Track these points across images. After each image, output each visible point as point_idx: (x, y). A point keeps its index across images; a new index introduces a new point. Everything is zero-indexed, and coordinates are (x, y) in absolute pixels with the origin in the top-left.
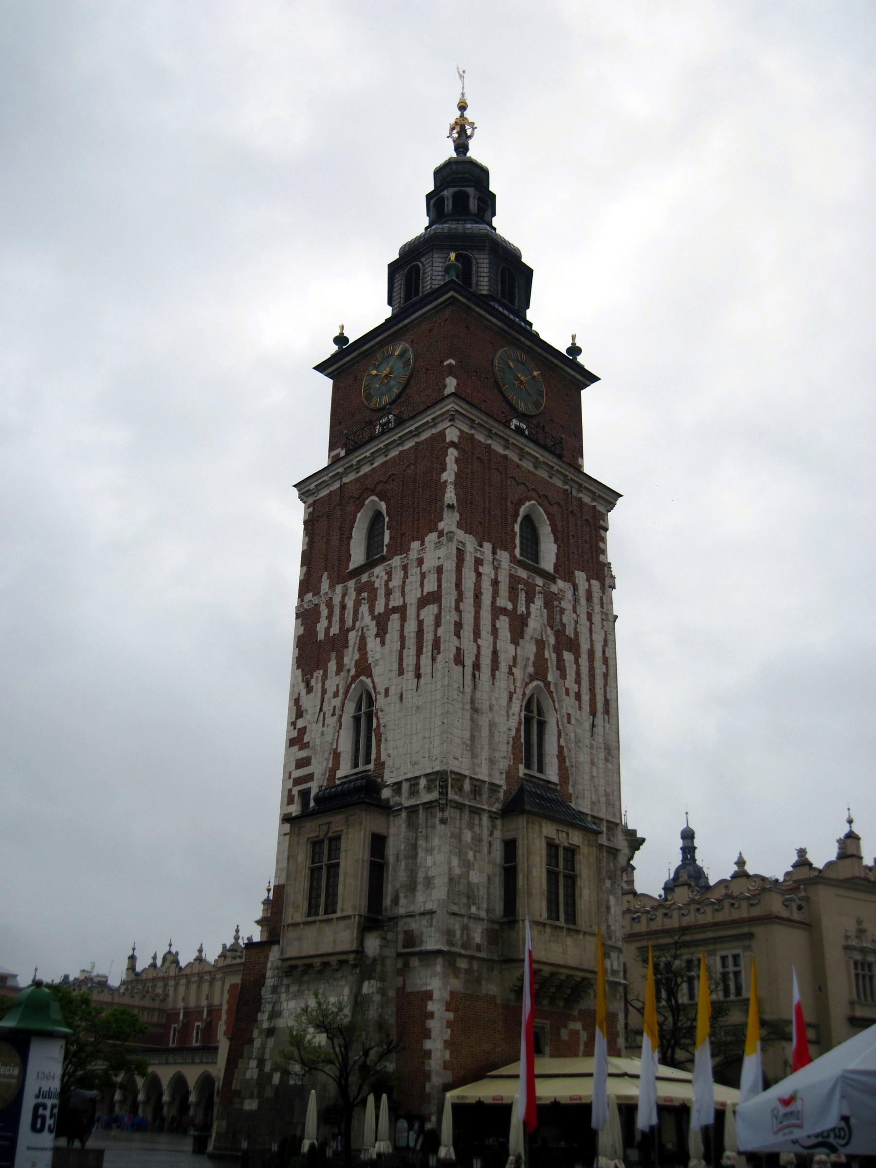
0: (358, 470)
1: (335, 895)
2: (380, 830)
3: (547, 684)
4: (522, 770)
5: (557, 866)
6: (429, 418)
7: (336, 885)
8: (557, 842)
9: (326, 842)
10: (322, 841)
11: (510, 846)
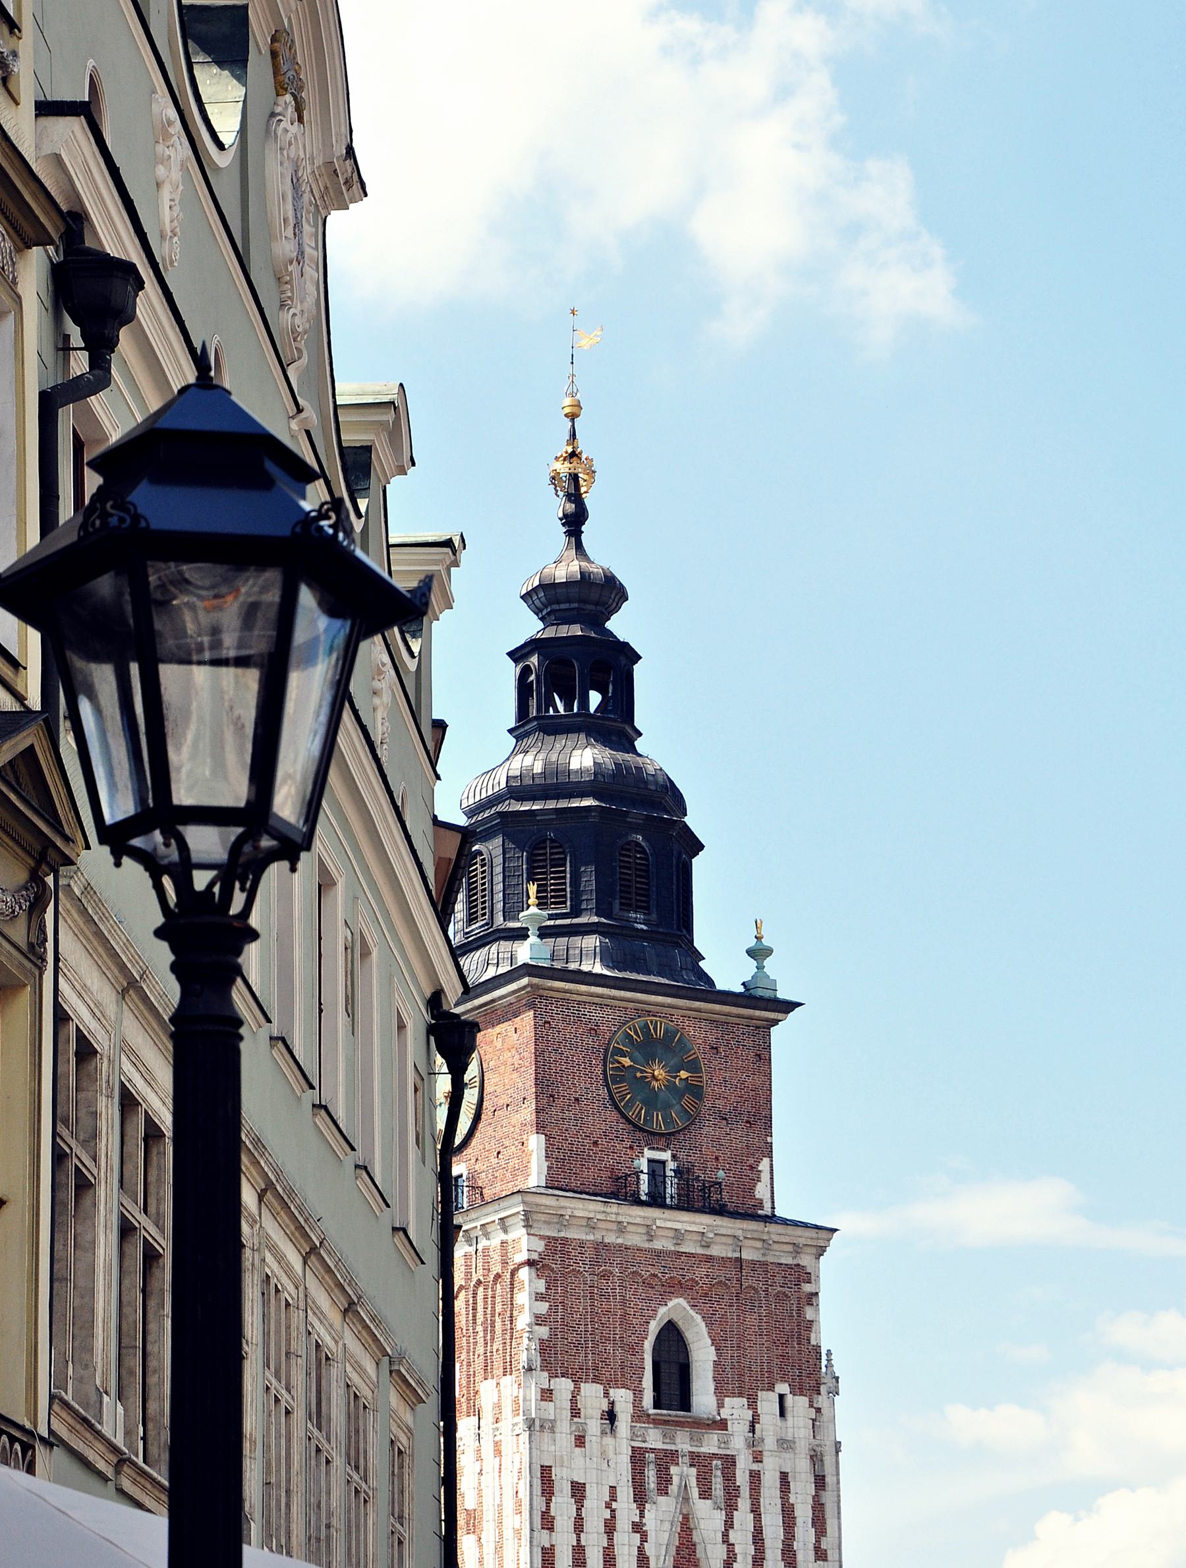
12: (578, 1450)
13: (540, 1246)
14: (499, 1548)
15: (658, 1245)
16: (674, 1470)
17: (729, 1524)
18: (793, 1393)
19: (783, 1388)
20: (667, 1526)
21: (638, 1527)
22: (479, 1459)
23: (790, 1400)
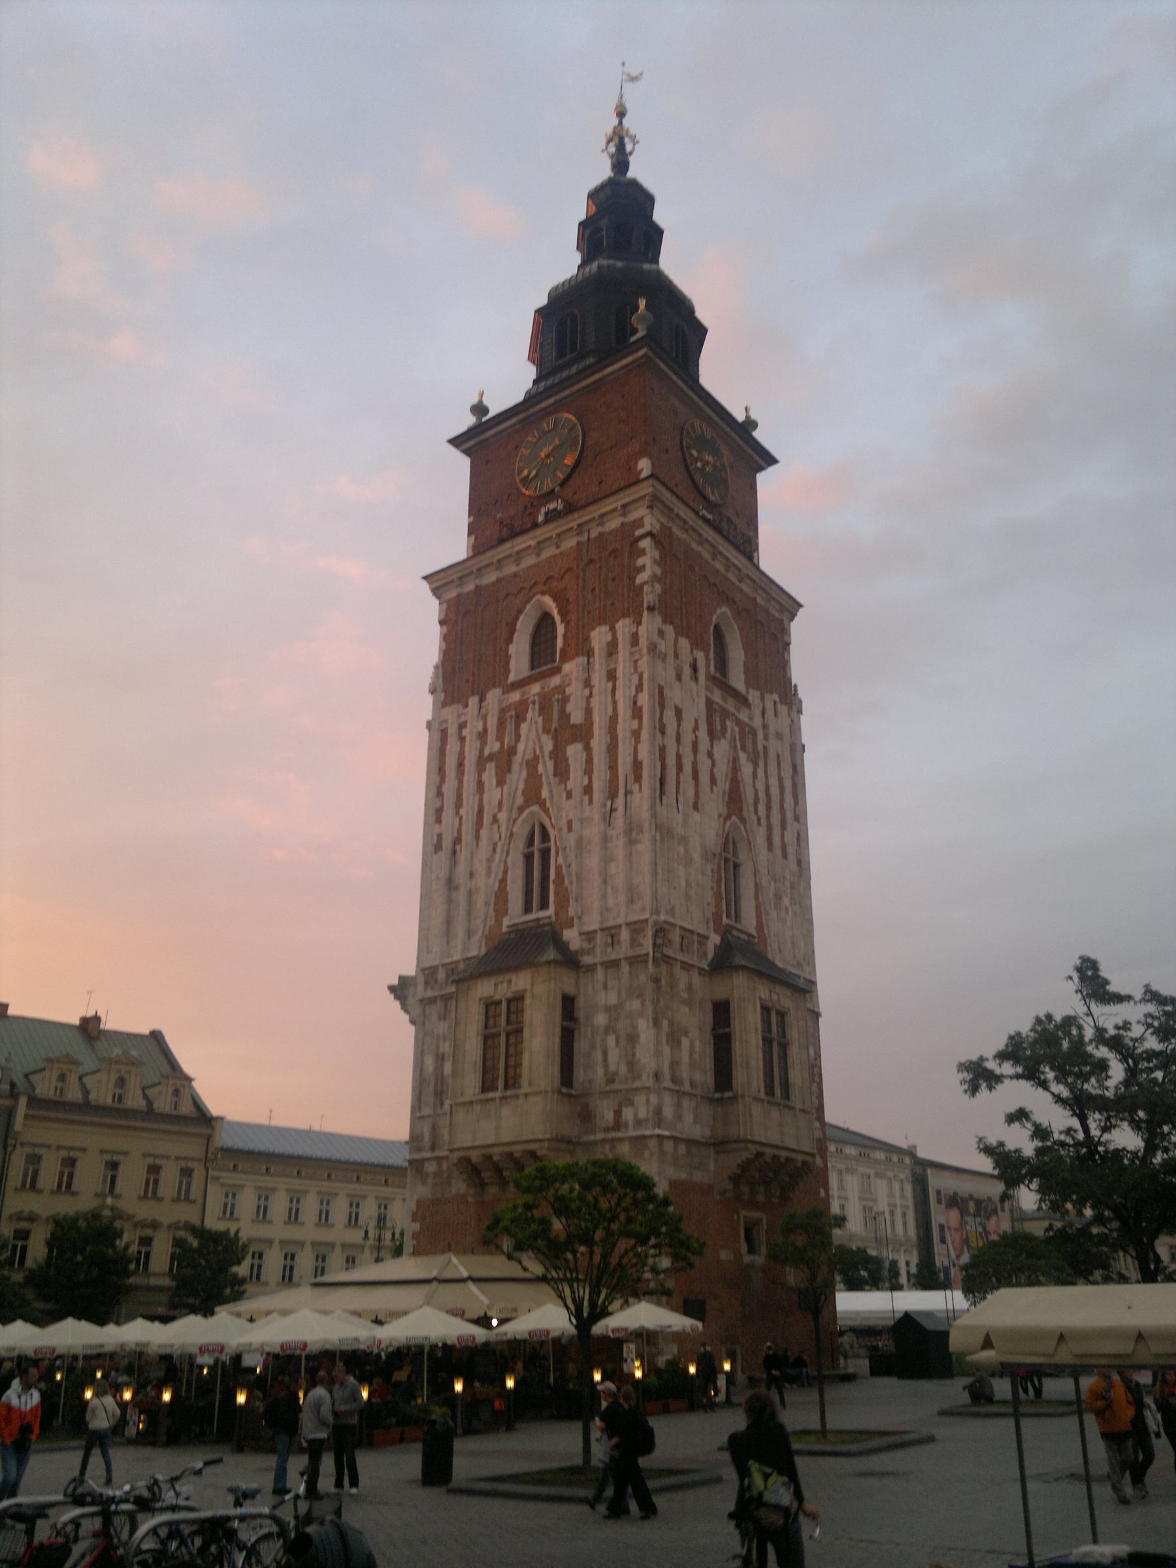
0: (518, 561)
1: (518, 1065)
2: (570, 990)
3: (743, 821)
4: (725, 920)
5: (770, 1031)
6: (618, 504)
7: (519, 1054)
8: (769, 1004)
9: (504, 1004)
10: (499, 1003)
11: (722, 1012)
12: (677, 683)
13: (658, 527)
14: (612, 749)
15: (718, 565)
16: (728, 723)
17: (755, 776)
18: (781, 702)
19: (776, 697)
20: (725, 760)
21: (710, 755)
22: (588, 683)
23: (779, 706)
